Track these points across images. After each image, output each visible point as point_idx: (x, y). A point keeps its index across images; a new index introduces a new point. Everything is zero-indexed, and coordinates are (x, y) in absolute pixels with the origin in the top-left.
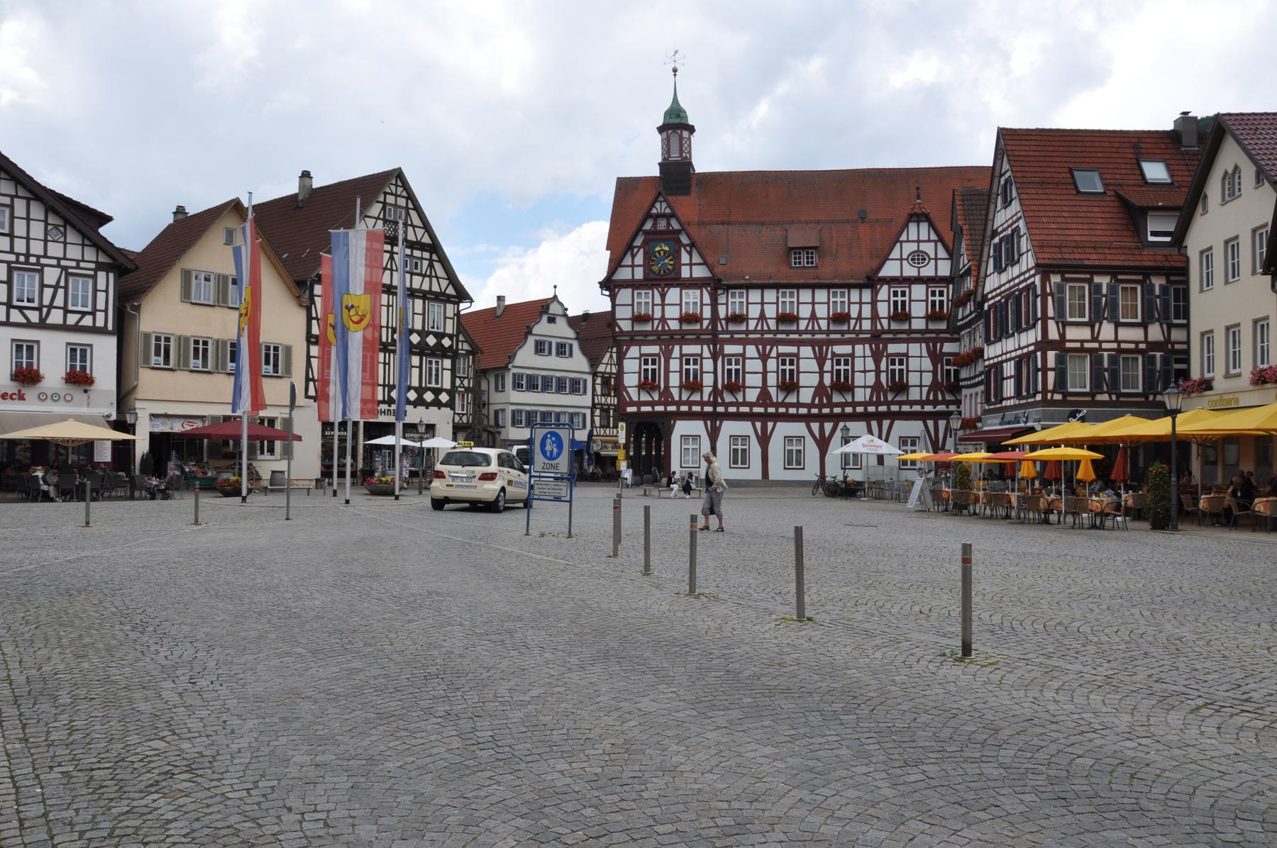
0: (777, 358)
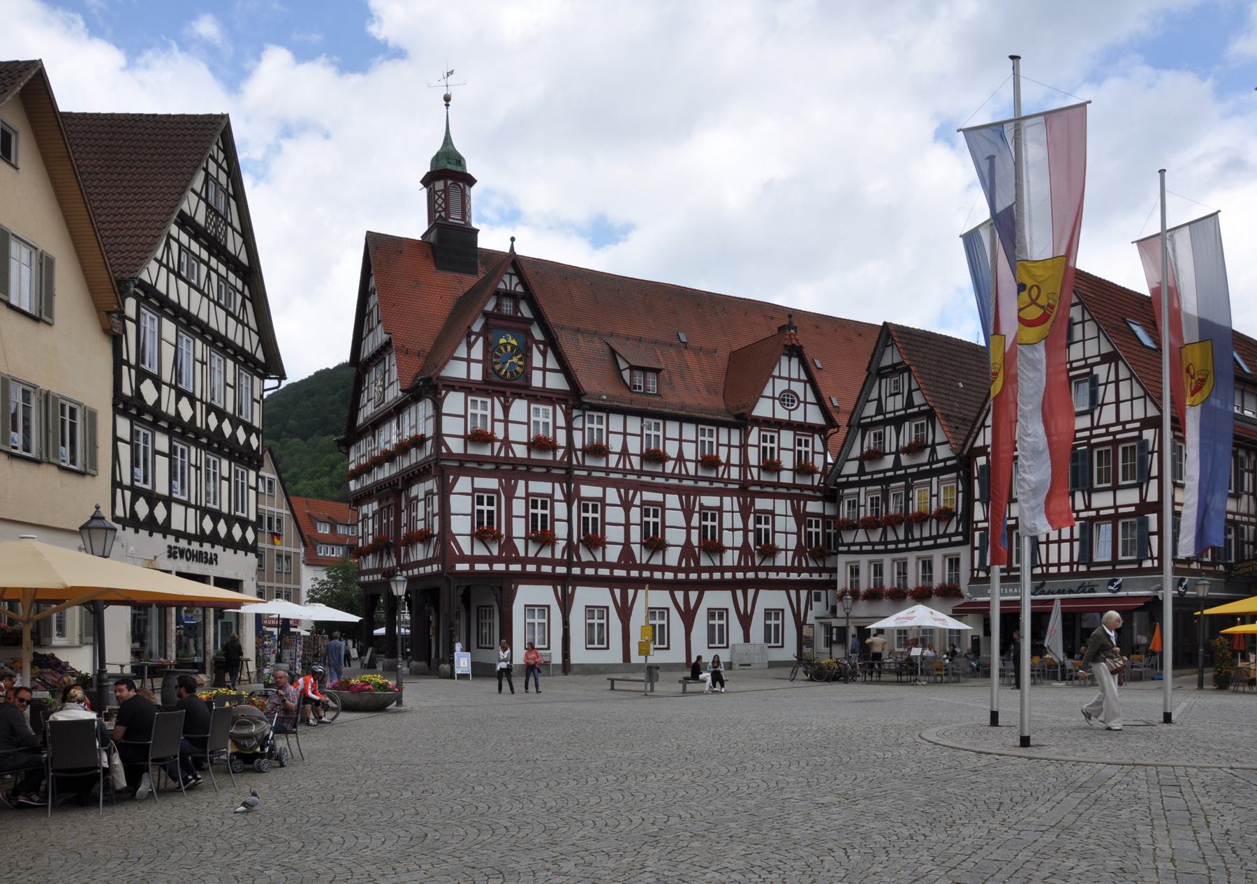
0: (640, 507)
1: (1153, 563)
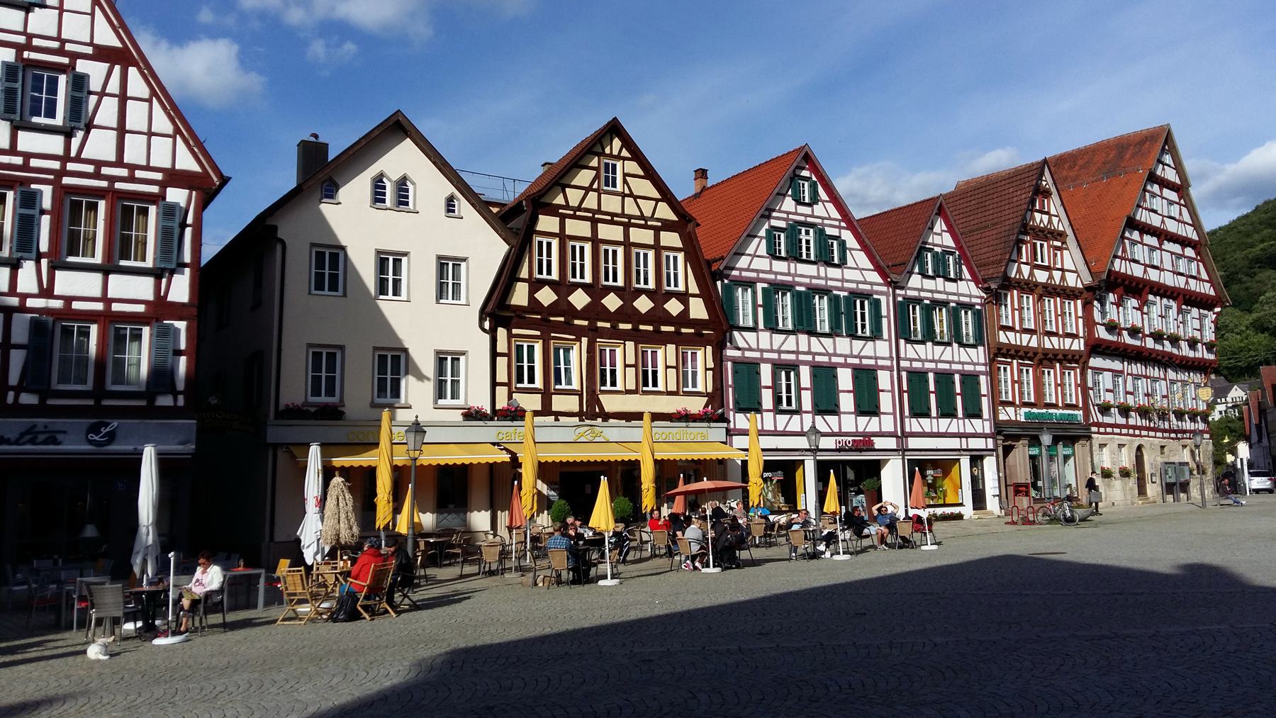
1: (175, 400)
